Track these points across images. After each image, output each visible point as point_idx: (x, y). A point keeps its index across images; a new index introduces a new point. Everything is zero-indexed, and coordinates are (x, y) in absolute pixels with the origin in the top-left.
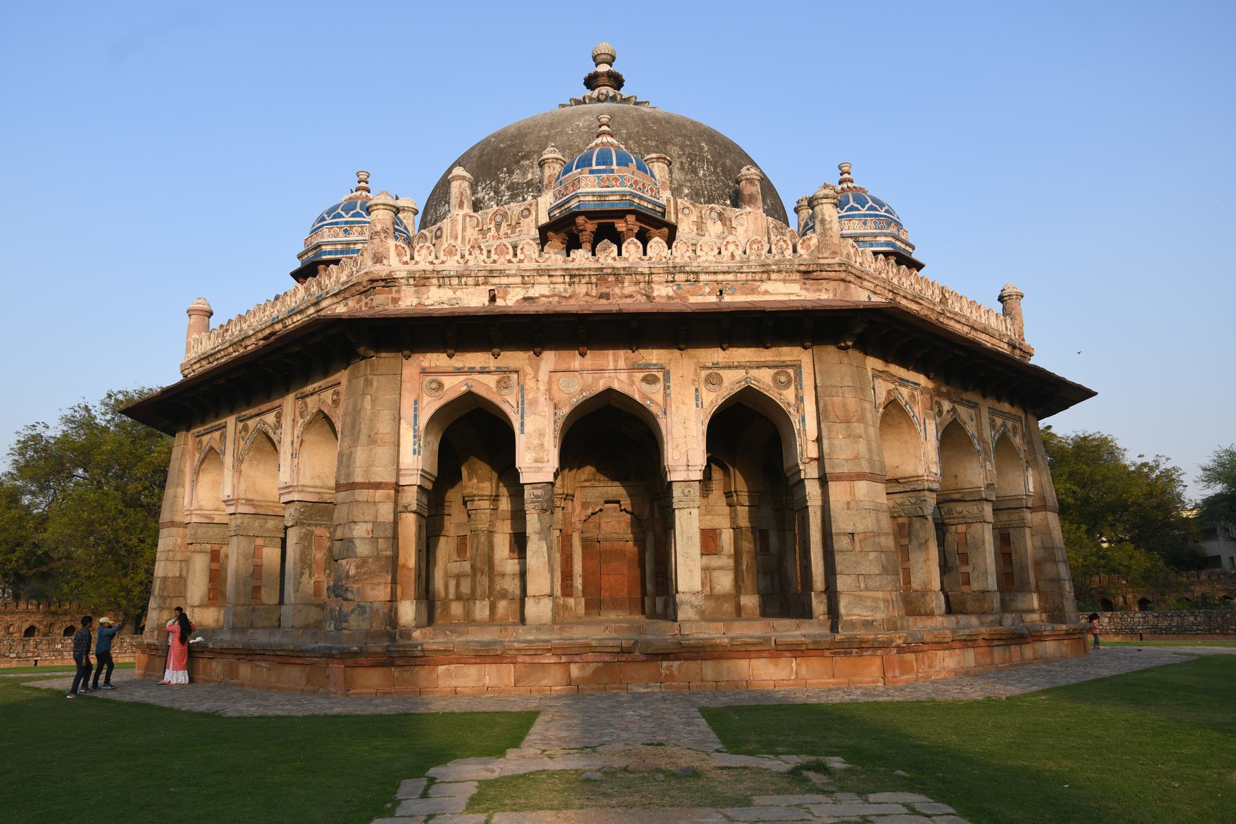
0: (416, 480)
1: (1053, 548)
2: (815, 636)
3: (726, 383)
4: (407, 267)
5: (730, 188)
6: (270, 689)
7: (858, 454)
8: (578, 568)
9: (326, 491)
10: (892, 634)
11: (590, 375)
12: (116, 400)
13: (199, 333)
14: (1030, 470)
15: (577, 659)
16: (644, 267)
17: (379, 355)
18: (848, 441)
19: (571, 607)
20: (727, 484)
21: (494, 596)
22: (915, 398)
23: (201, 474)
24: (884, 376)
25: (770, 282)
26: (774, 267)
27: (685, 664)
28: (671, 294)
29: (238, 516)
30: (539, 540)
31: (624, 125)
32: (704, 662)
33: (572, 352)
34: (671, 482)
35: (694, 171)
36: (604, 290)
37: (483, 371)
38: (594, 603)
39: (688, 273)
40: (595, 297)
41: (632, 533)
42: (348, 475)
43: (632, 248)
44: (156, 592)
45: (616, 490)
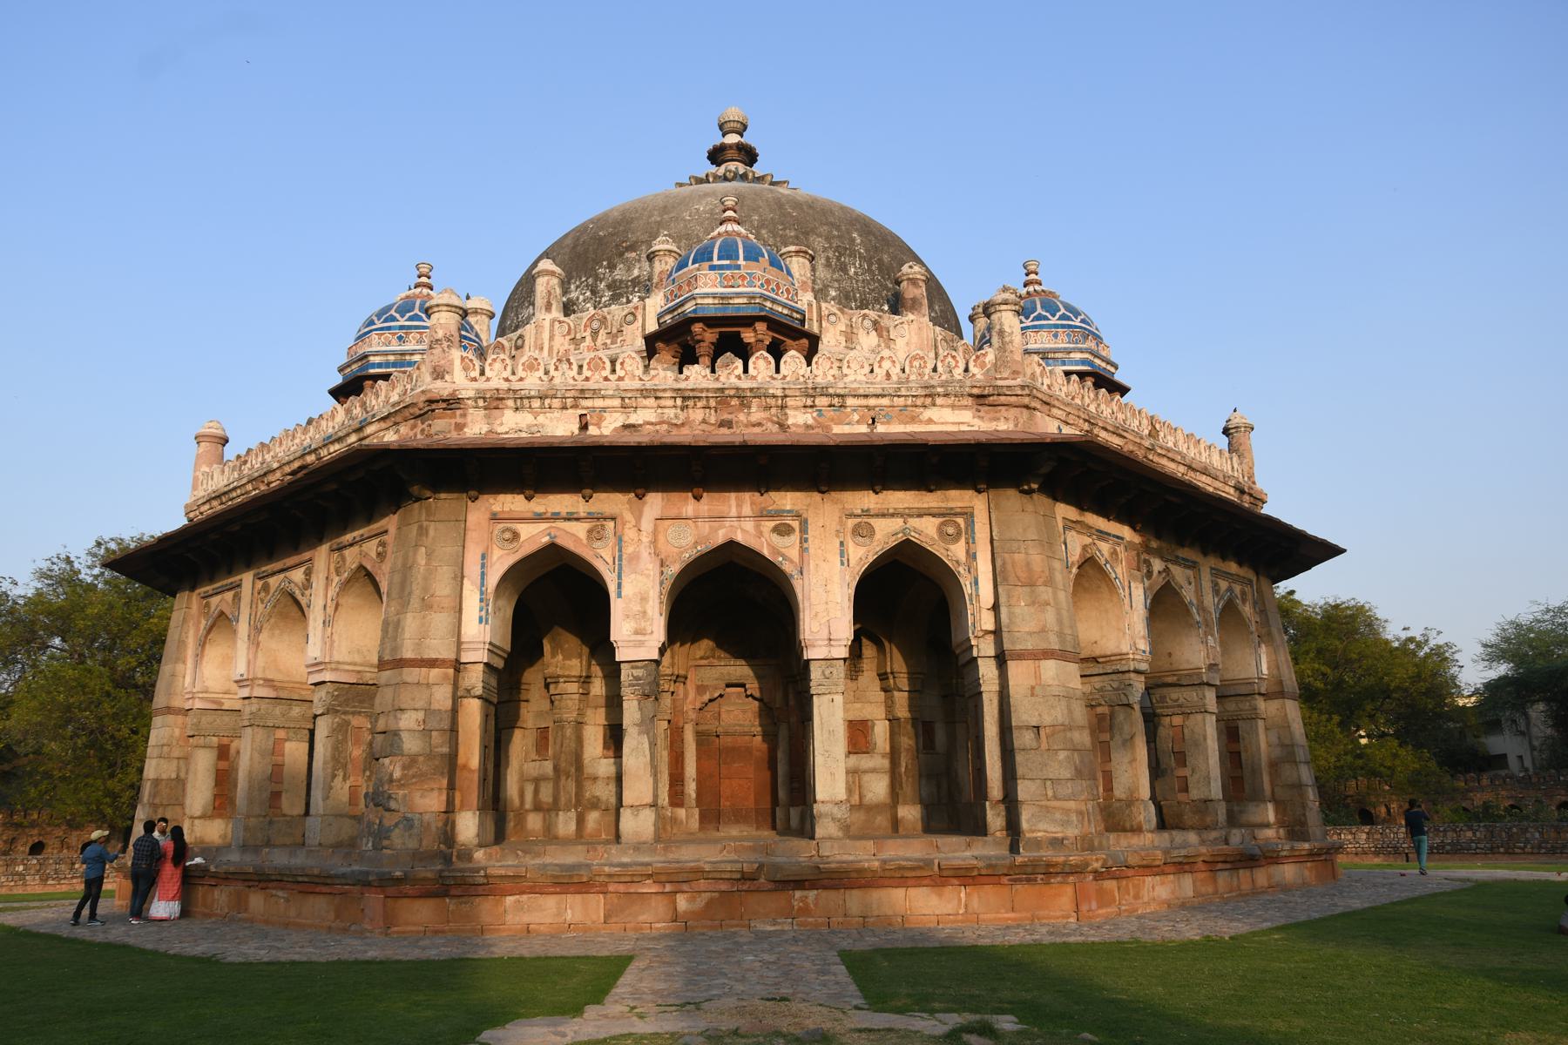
0: (483, 656)
1: (1293, 746)
2: (989, 858)
3: (878, 536)
4: (475, 385)
5: (888, 290)
6: (287, 925)
7: (1045, 626)
8: (691, 769)
9: (367, 669)
10: (1087, 855)
11: (707, 525)
12: (107, 549)
13: (210, 465)
14: (1263, 646)
15: (685, 887)
16: (776, 388)
17: (437, 496)
18: (1033, 610)
19: (682, 821)
20: (881, 663)
21: (583, 805)
22: (1117, 554)
23: (207, 646)
24: (1078, 527)
25: (935, 409)
26: (940, 390)
27: (824, 894)
28: (810, 422)
29: (253, 700)
30: (639, 734)
31: (755, 210)
32: (848, 892)
33: (684, 494)
35: (843, 269)
36: (726, 416)
37: (570, 518)
38: (712, 815)
39: (831, 395)
40: (713, 425)
41: (761, 725)
42: (395, 649)
43: (761, 364)
44: (145, 799)
45: (740, 670)
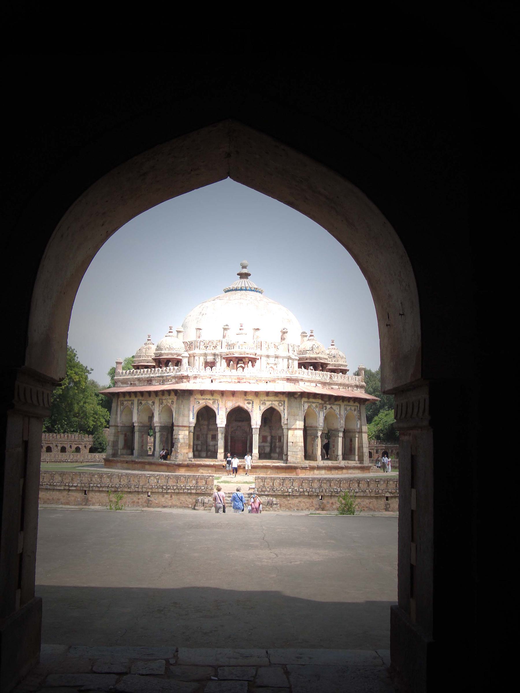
8: (229, 444)
16: (248, 376)
30: (221, 440)
34: (252, 428)
37: (209, 399)
44: (110, 445)
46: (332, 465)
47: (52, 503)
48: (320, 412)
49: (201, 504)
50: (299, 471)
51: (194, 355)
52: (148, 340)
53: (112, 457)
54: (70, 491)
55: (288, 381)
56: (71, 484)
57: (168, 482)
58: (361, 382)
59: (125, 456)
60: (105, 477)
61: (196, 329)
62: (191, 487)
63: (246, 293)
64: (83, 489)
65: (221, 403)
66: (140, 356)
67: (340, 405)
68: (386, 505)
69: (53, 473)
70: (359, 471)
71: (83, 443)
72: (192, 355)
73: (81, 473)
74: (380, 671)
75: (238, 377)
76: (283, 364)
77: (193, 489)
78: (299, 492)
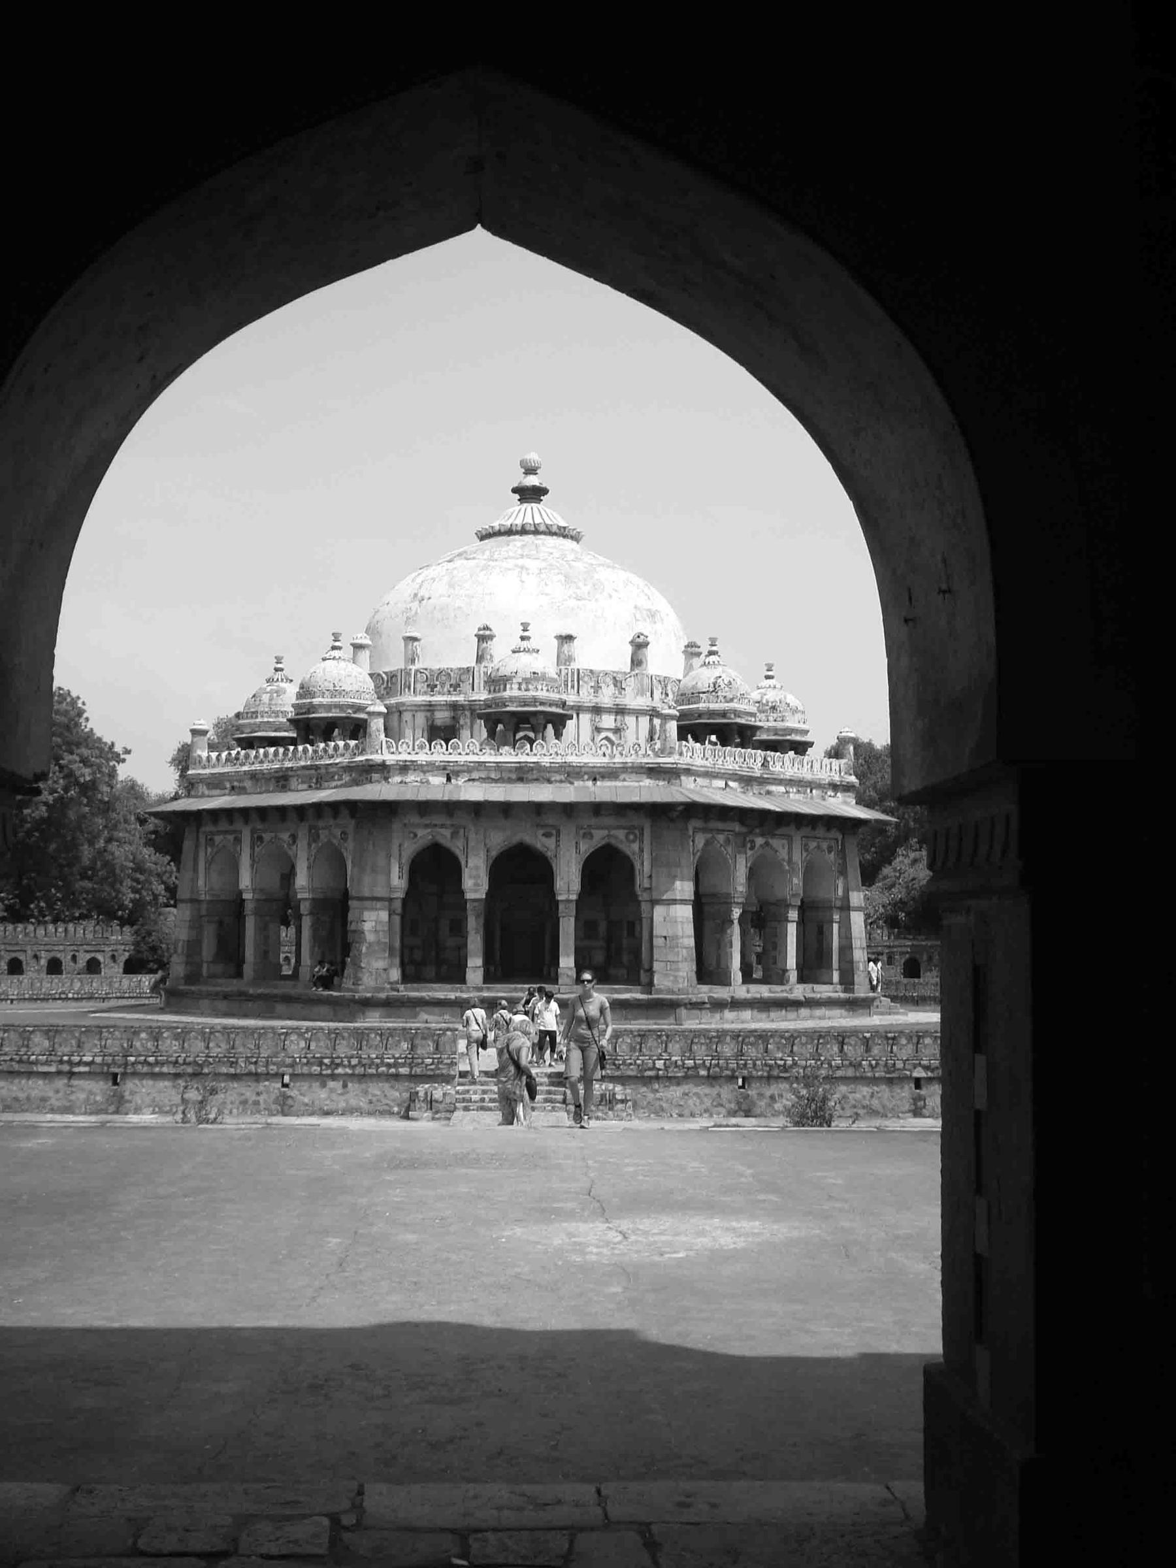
8: (497, 945)
16: (546, 761)
22: (729, 841)
28: (563, 779)
30: (476, 933)
36: (521, 775)
37: (442, 826)
44: (180, 951)
46: (772, 995)
47: (27, 1111)
48: (738, 856)
49: (423, 1105)
50: (683, 1012)
51: (401, 709)
52: (277, 670)
53: (186, 984)
54: (73, 1077)
55: (650, 774)
56: (76, 1059)
57: (337, 1048)
58: (845, 776)
59: (220, 981)
60: (166, 1038)
61: (403, 638)
62: (398, 1058)
63: (536, 542)
64: (108, 1069)
65: (474, 836)
66: (255, 714)
67: (789, 838)
68: (913, 1099)
69: (28, 1029)
70: (843, 1011)
71: (106, 949)
72: (394, 710)
73: (107, 1027)
74: (896, 1537)
75: (518, 765)
76: (634, 730)
77: (403, 1065)
78: (684, 1068)
